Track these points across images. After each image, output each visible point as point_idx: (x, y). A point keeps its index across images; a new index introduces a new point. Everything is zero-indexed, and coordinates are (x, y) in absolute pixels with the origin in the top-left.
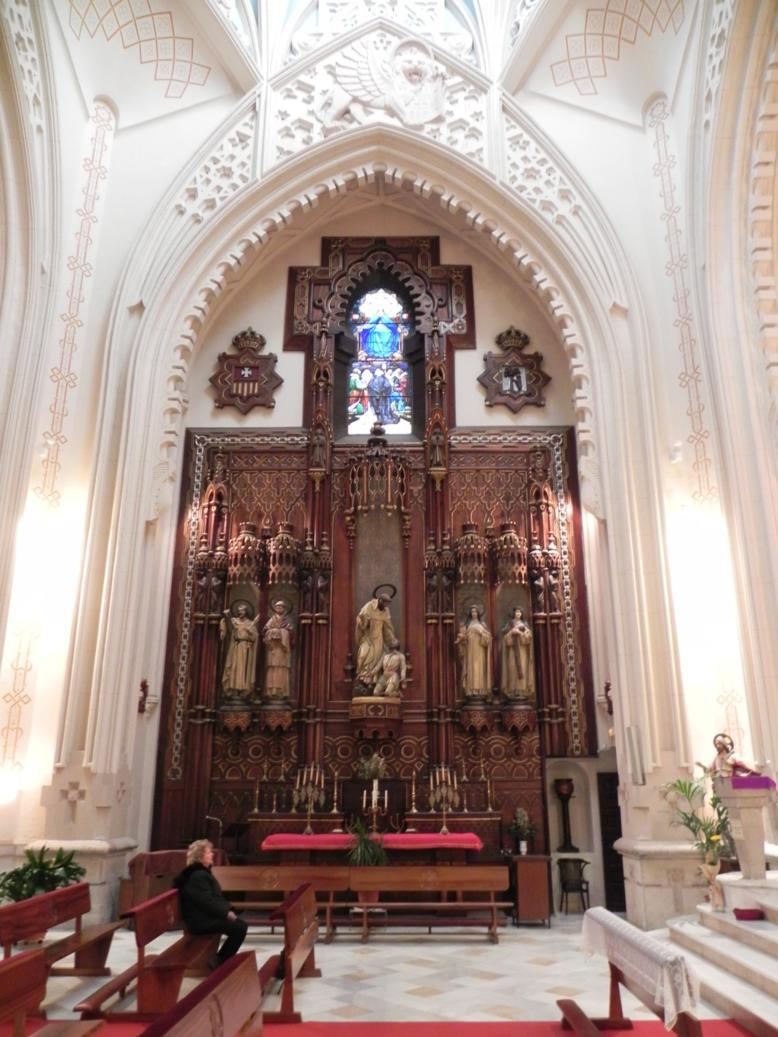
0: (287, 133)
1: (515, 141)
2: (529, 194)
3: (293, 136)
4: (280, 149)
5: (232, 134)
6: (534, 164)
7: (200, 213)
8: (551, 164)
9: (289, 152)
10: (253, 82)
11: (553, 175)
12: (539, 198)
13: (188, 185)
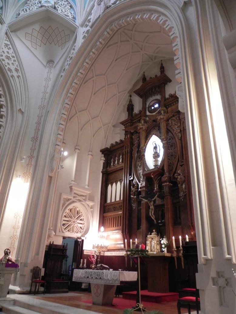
1: (6, 45)
2: (5, 63)
6: (10, 55)
8: (16, 59)
11: (15, 63)
12: (8, 66)
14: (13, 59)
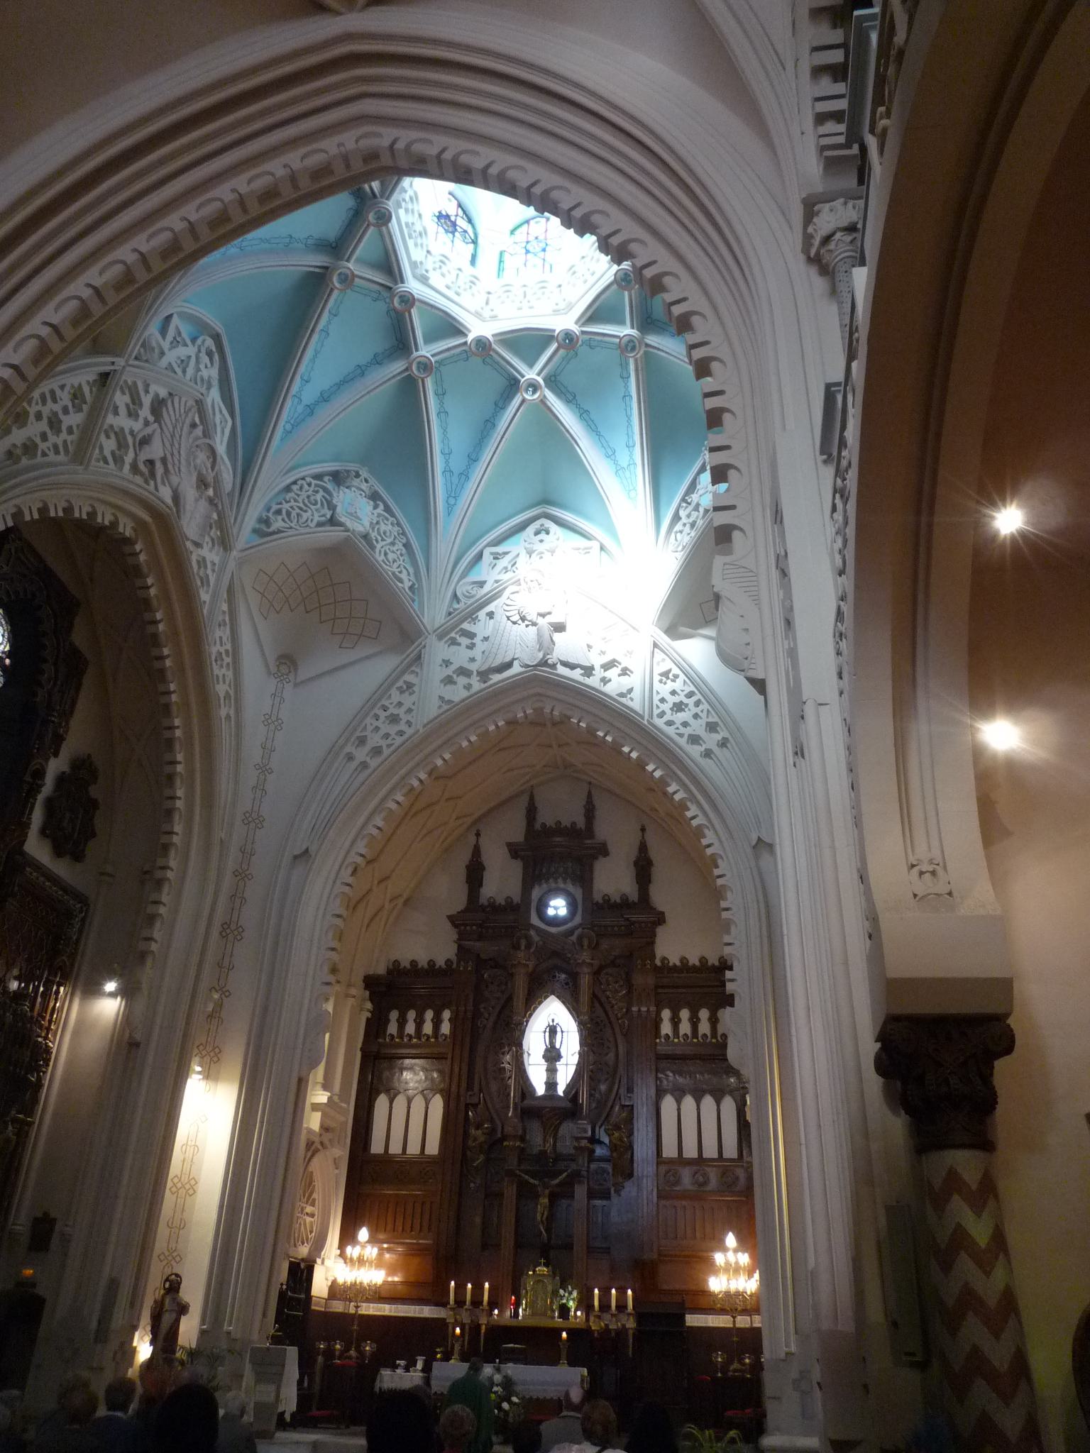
0: (449, 681)
3: (455, 683)
4: (441, 698)
5: (400, 683)
7: (368, 759)
9: (450, 702)
10: (419, 633)
11: (701, 707)
12: (687, 731)
13: (358, 734)
14: (691, 701)
